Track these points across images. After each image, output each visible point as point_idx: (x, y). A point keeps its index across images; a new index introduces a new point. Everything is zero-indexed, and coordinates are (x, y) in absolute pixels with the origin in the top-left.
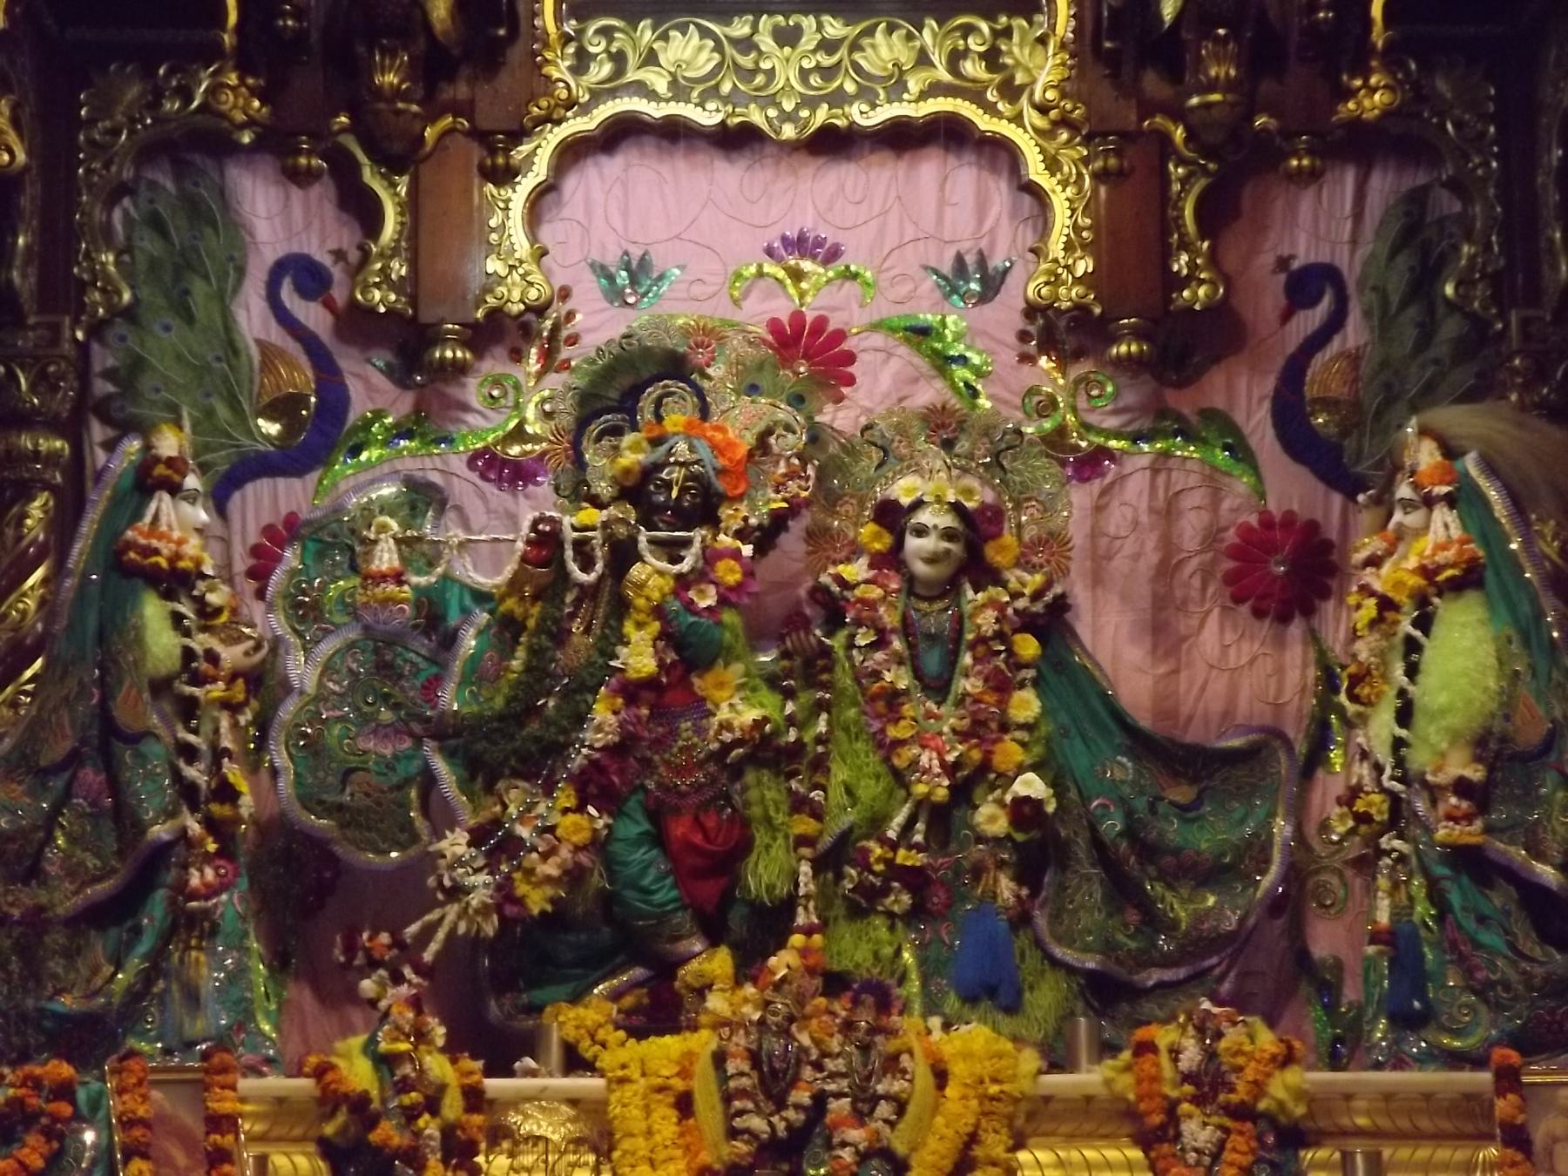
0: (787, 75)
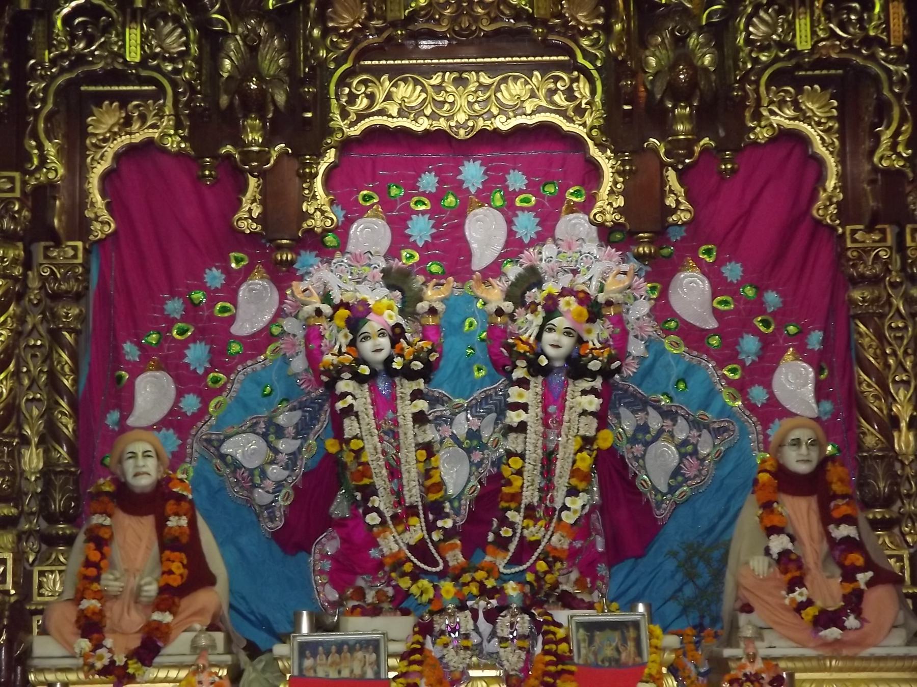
0: (462, 102)
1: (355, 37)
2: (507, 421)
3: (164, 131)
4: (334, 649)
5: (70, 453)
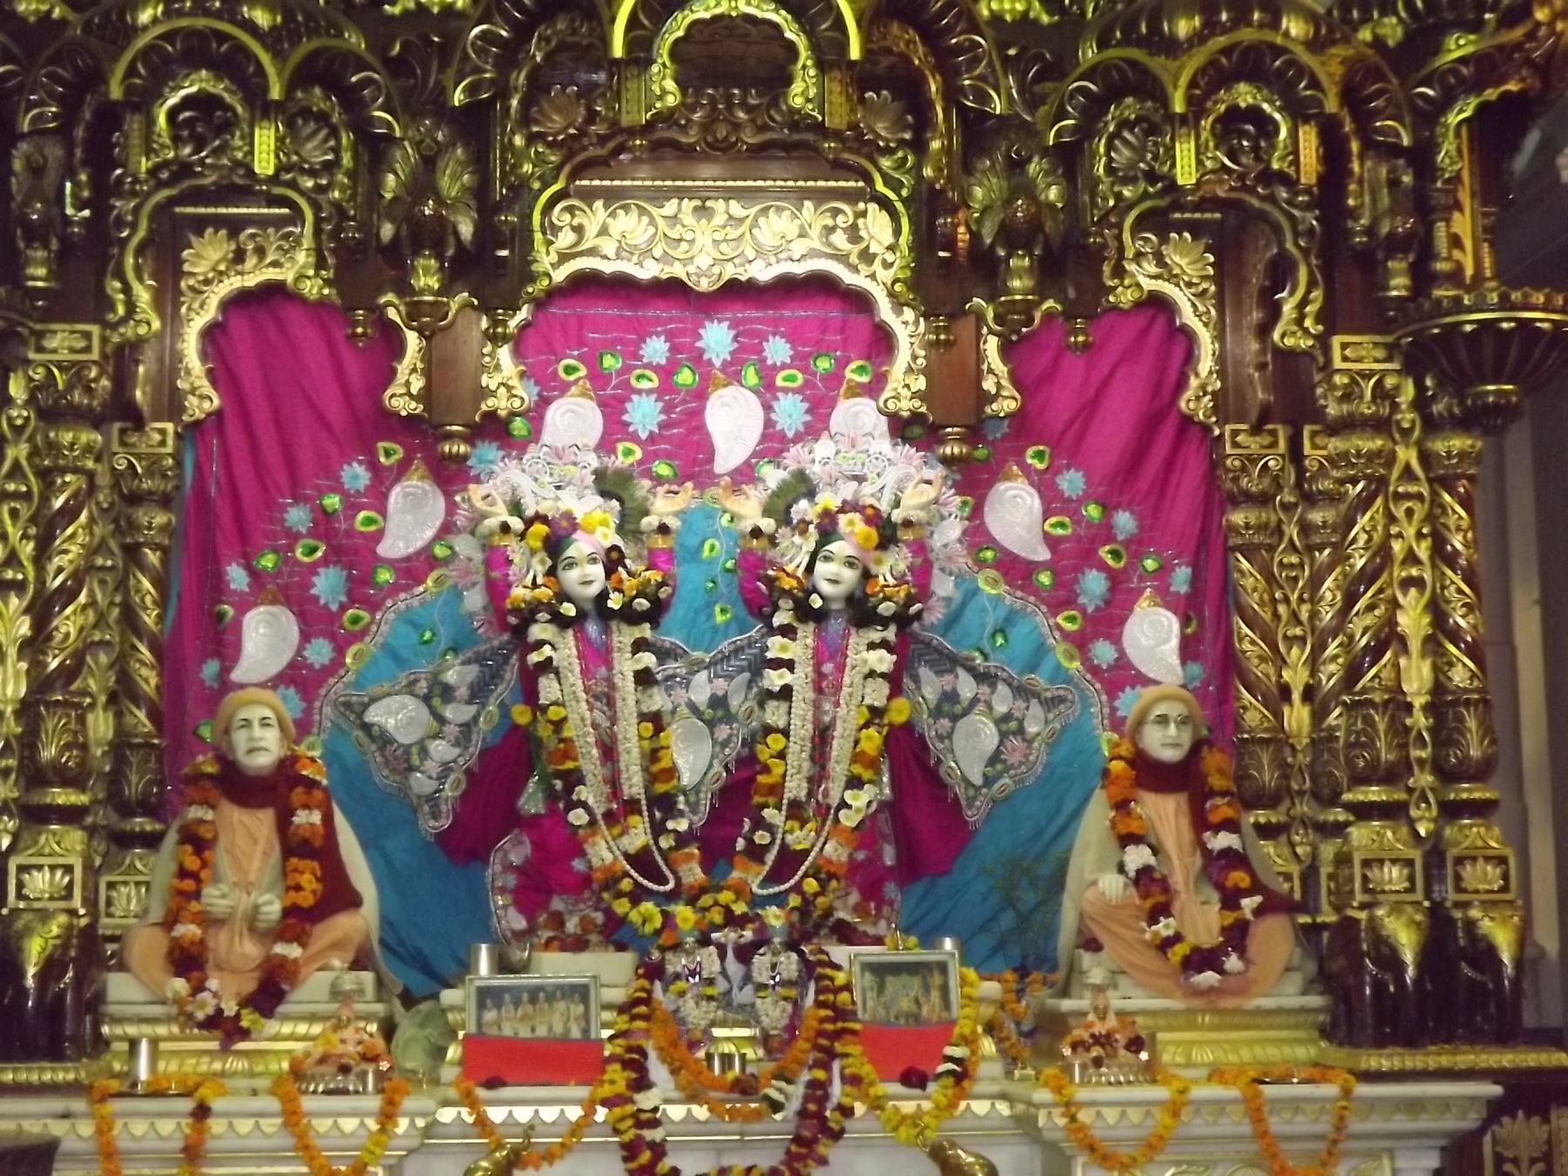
1: (569, 147)
2: (766, 684)
3: (297, 267)
4: (525, 997)
5: (150, 716)
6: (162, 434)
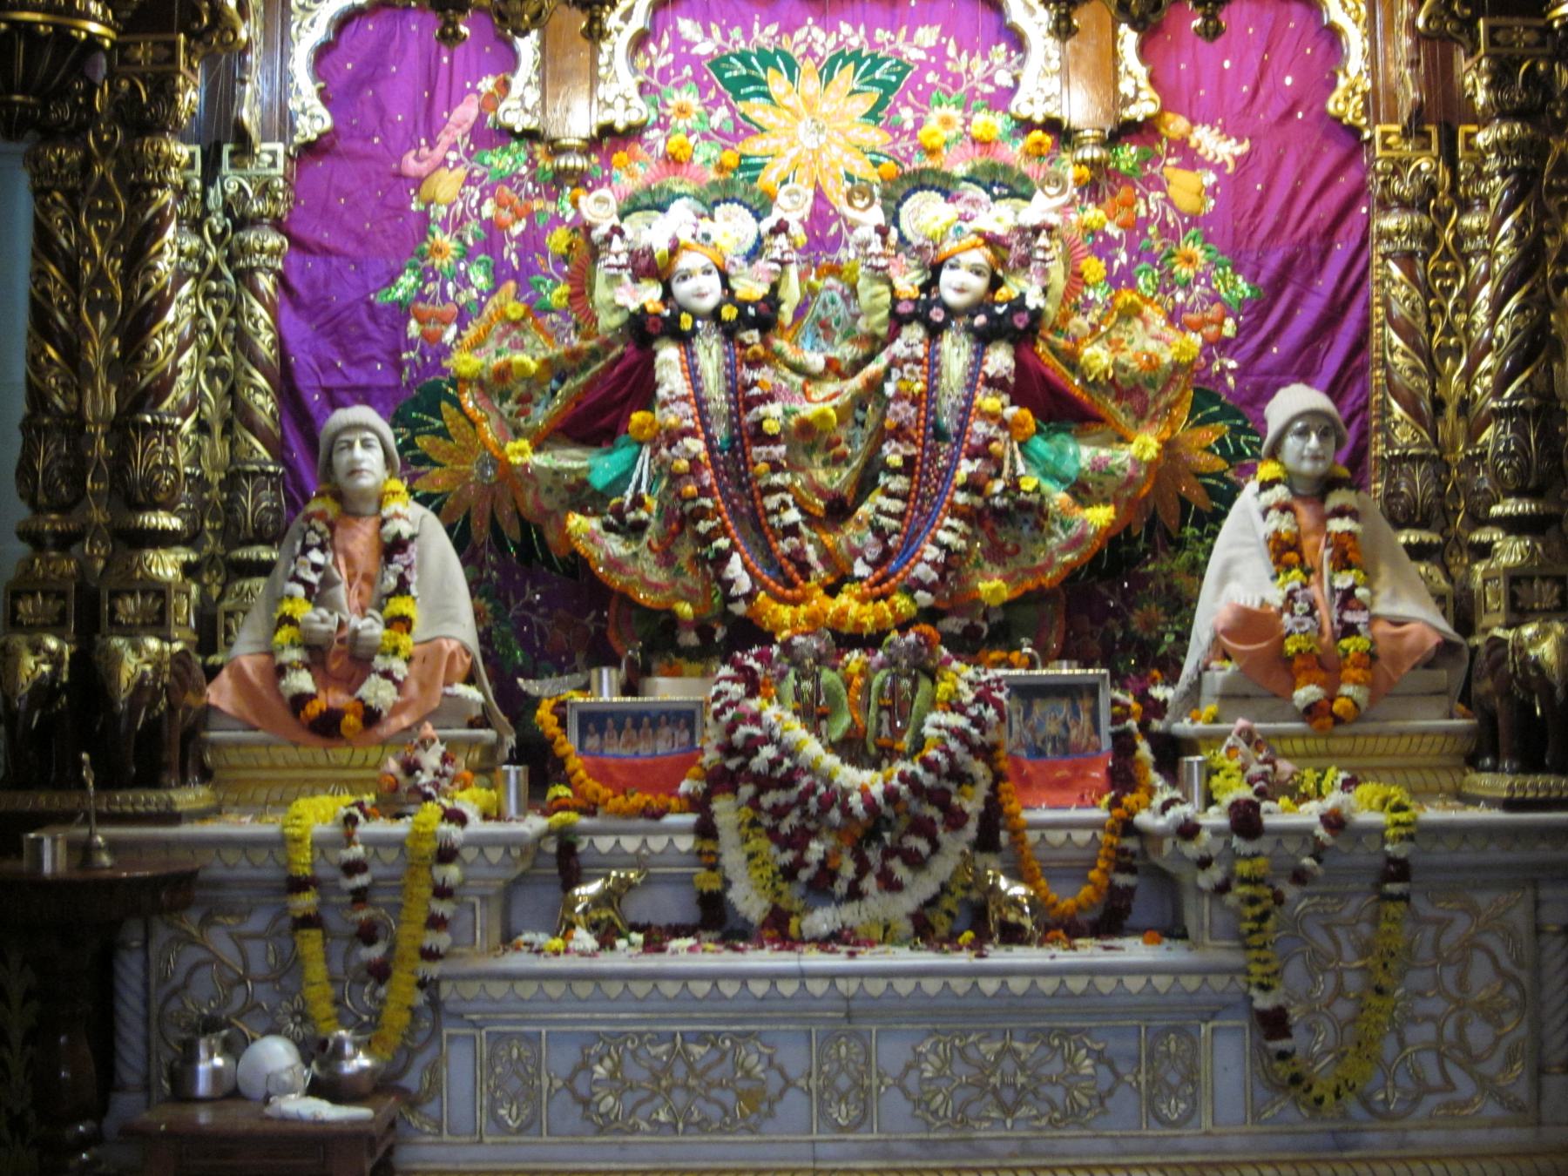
6: (271, 156)
